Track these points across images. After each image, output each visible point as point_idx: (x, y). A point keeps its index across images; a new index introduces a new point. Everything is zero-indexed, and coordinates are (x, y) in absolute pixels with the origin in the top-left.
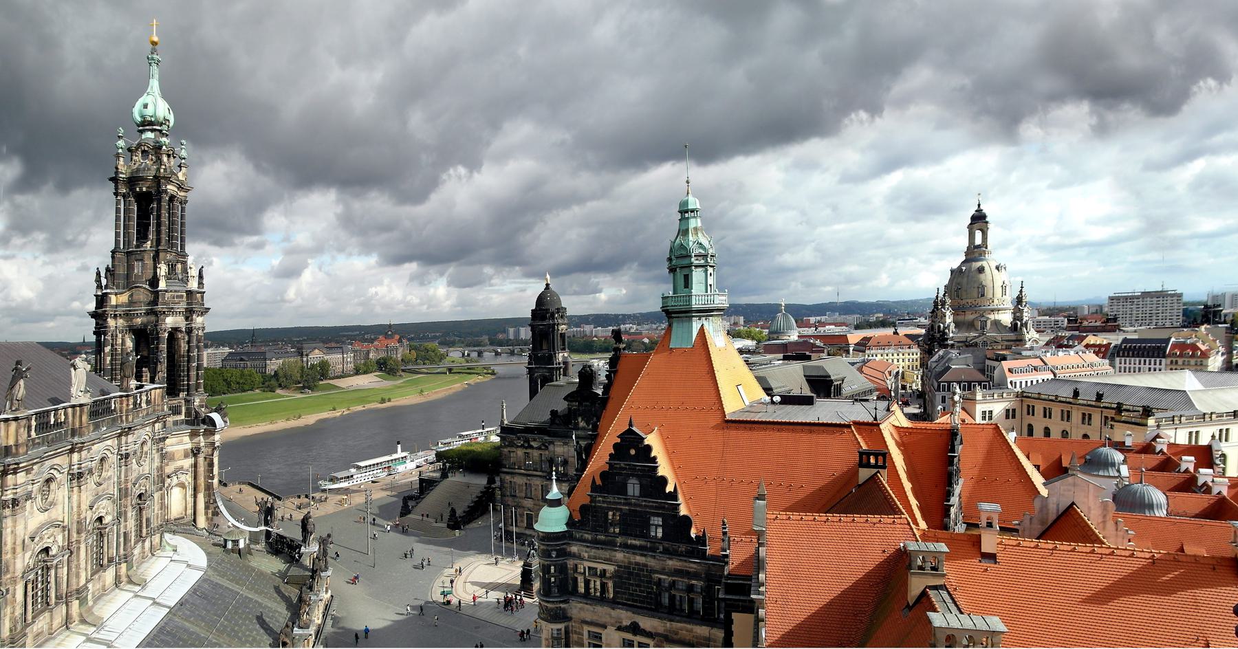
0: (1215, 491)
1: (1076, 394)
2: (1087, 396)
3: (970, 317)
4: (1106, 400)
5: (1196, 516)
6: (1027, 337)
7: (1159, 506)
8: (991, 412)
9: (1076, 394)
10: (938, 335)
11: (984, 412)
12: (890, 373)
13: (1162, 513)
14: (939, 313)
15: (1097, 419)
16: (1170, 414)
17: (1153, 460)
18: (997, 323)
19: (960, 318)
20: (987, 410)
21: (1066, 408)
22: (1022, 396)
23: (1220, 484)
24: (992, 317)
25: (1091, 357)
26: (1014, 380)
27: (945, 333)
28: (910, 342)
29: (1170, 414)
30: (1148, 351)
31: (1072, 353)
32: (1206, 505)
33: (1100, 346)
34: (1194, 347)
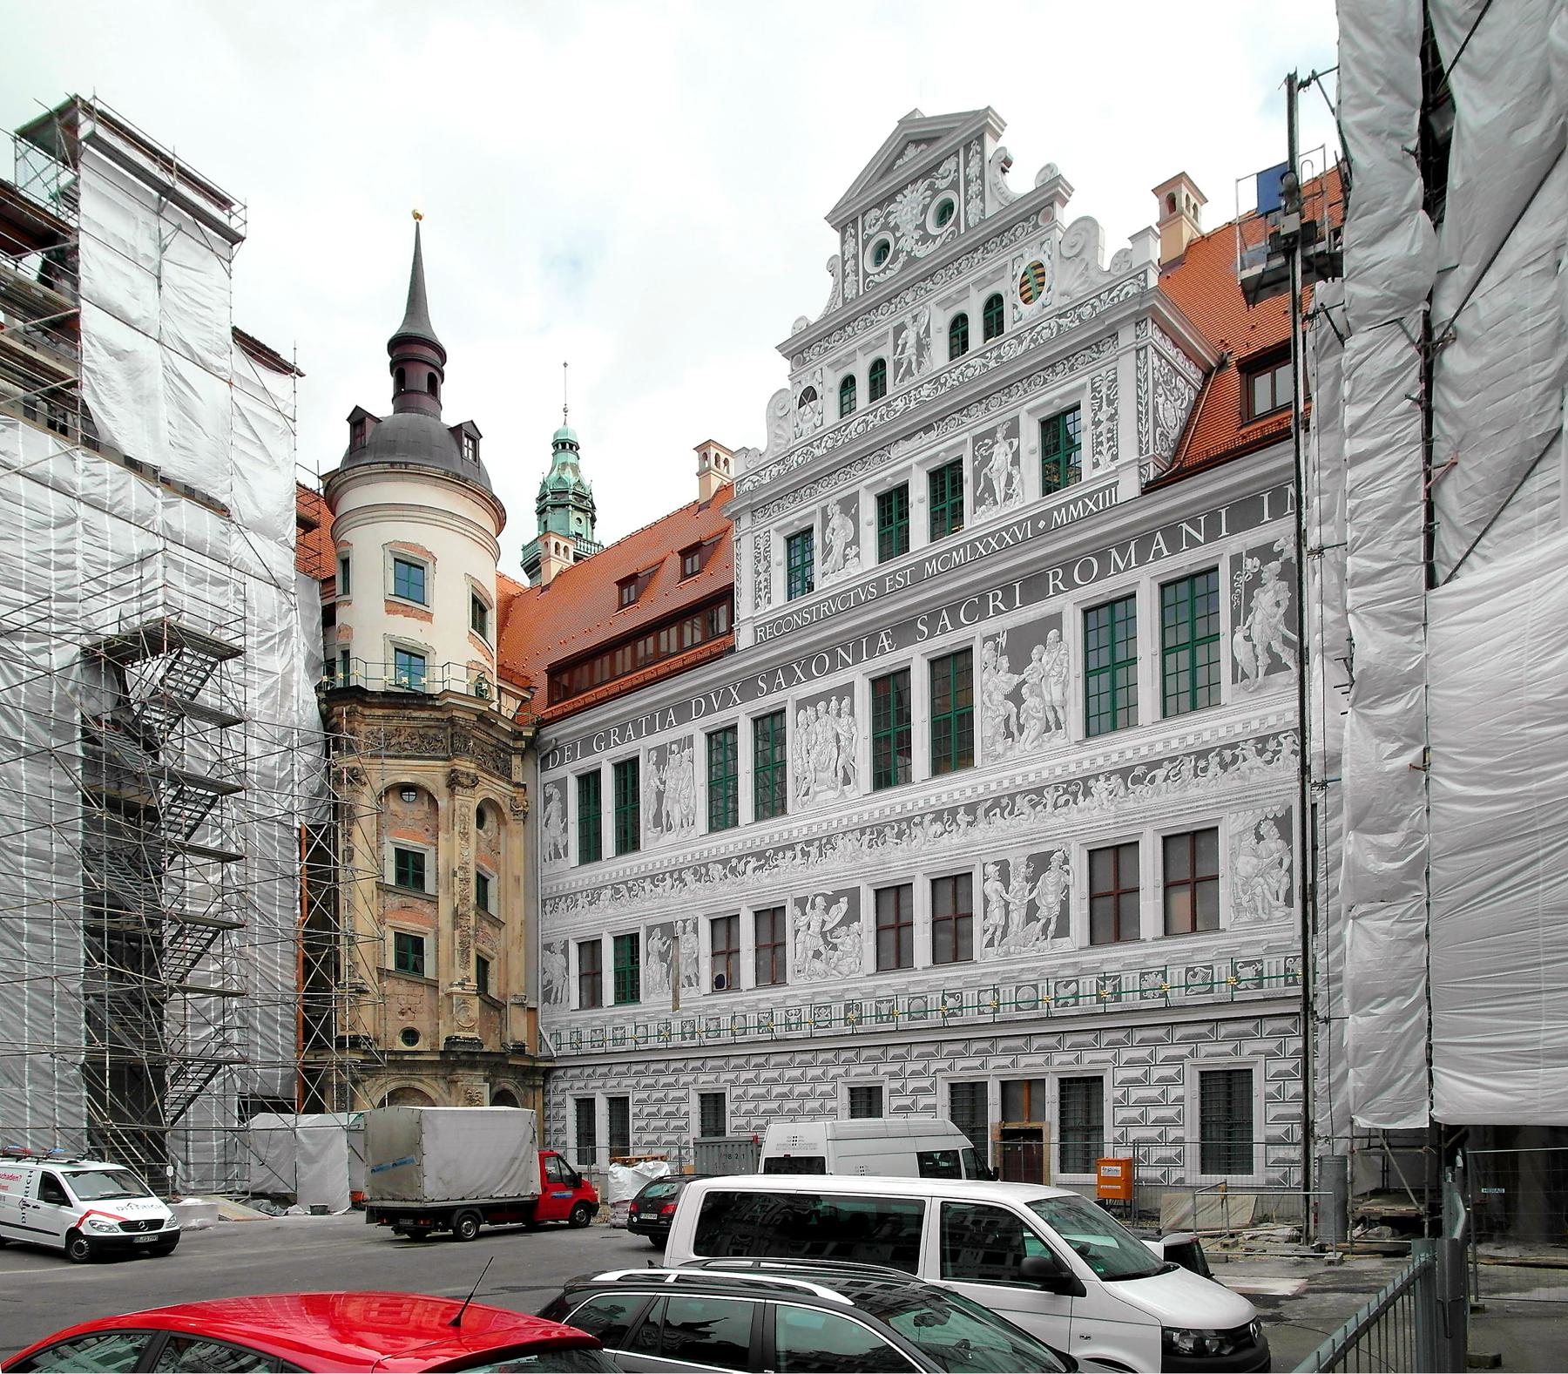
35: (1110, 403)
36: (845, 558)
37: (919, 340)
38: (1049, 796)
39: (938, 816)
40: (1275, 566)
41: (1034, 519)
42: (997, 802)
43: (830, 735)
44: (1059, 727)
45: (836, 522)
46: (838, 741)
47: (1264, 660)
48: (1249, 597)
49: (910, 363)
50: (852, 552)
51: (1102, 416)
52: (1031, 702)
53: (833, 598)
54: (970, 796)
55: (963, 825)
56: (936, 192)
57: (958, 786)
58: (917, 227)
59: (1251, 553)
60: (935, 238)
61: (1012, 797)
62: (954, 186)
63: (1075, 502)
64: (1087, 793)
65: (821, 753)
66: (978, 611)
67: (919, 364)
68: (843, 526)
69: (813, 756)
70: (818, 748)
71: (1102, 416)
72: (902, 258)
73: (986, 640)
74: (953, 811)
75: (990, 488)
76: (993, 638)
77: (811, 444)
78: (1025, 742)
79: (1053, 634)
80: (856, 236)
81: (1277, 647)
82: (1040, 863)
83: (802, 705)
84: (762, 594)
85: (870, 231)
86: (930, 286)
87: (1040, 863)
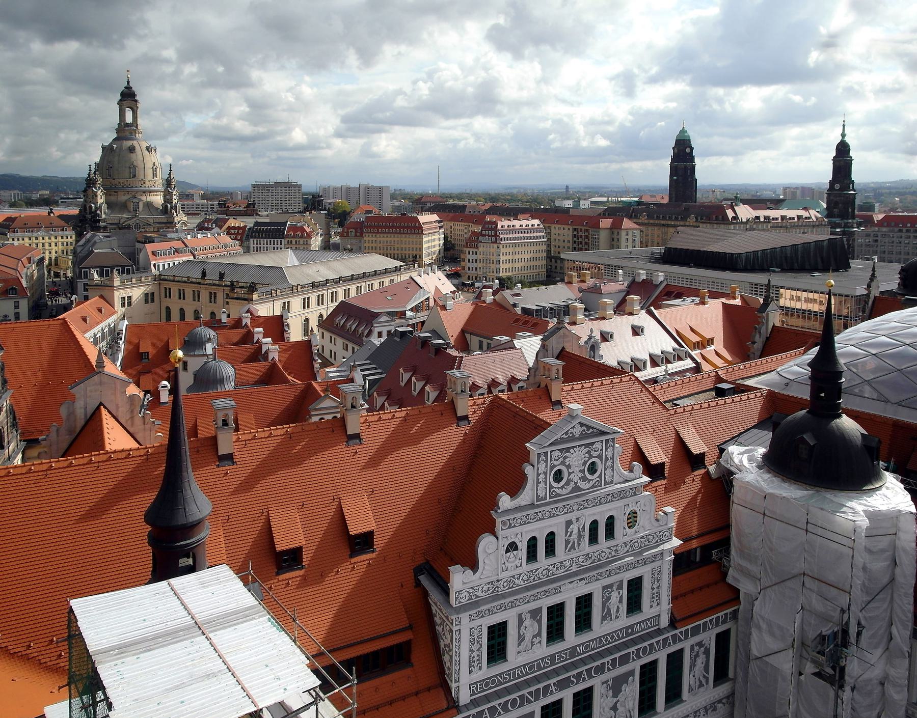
0: (270, 358)
1: (204, 274)
2: (213, 276)
4: (227, 279)
6: (177, 219)
7: (229, 380)
8: (130, 298)
9: (204, 274)
10: (89, 216)
11: (123, 299)
12: (29, 260)
15: (220, 296)
16: (268, 289)
17: (238, 333)
20: (126, 295)
21: (196, 288)
22: (160, 279)
23: (273, 351)
24: (144, 198)
25: (227, 239)
28: (63, 223)
29: (268, 289)
30: (273, 233)
31: (209, 235)
33: (239, 228)
34: (302, 229)
35: (658, 581)
36: (532, 645)
37: (579, 532)
40: (702, 649)
41: (627, 628)
45: (527, 622)
47: (698, 683)
49: (574, 543)
50: (536, 640)
52: (621, 709)
53: (524, 666)
56: (591, 457)
58: (580, 471)
60: (589, 481)
62: (600, 457)
63: (643, 621)
66: (600, 670)
67: (579, 545)
68: (532, 626)
71: (655, 586)
72: (572, 485)
73: (603, 683)
75: (609, 613)
76: (606, 682)
77: (513, 577)
79: (631, 678)
80: (546, 462)
84: (475, 664)
85: (556, 463)
86: (586, 505)
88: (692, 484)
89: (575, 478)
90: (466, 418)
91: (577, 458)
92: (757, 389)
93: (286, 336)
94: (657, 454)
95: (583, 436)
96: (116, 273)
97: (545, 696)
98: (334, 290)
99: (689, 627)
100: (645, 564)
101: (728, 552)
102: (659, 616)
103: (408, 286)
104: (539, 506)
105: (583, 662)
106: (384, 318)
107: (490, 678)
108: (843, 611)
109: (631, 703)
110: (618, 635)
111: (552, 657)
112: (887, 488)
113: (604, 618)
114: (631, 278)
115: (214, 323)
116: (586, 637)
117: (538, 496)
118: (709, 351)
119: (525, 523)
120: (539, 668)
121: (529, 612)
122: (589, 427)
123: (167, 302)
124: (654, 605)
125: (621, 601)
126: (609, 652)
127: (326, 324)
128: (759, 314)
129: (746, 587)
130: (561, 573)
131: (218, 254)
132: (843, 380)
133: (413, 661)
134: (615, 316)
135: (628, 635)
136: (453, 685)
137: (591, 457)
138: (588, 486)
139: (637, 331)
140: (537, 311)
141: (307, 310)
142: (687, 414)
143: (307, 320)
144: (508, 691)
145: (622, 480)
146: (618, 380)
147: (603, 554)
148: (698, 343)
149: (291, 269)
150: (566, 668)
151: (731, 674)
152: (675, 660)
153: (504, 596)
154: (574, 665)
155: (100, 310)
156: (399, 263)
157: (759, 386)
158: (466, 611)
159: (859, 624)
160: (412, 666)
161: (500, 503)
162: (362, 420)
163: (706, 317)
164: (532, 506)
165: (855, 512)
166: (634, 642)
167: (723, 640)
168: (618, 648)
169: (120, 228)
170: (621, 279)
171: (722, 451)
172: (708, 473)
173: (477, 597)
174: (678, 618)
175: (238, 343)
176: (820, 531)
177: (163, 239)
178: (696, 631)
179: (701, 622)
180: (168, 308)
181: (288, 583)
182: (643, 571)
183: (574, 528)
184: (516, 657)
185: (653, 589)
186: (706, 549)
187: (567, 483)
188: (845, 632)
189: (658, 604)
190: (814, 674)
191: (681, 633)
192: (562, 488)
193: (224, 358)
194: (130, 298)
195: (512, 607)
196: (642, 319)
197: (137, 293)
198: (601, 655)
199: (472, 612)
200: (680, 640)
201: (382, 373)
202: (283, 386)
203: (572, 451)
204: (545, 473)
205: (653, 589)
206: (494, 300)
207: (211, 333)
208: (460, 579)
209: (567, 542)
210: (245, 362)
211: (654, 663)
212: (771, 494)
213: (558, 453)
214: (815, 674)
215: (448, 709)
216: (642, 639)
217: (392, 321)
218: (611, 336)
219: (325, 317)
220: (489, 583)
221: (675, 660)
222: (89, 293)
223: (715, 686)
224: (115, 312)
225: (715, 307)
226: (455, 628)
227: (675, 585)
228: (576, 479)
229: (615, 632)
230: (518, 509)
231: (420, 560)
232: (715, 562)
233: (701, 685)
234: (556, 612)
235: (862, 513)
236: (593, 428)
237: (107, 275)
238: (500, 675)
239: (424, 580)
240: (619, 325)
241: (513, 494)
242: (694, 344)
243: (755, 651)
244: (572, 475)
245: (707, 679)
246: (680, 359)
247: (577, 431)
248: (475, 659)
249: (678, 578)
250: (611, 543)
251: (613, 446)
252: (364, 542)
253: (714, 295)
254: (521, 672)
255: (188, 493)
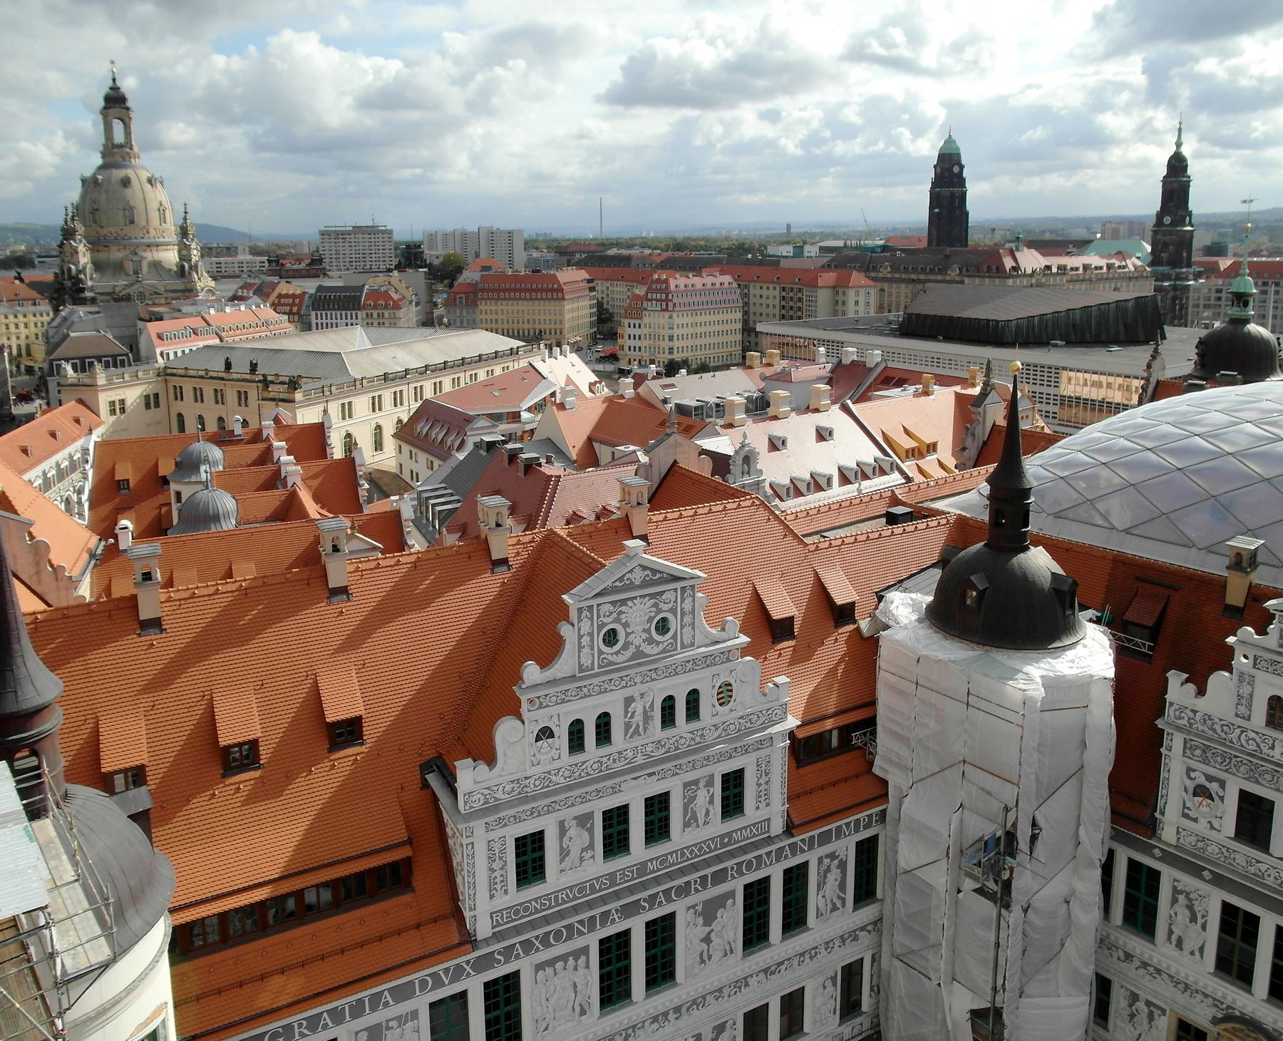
0: (289, 484)
1: (228, 365)
2: (240, 368)
3: (116, 254)
4: (260, 371)
5: (268, 520)
6: (199, 285)
7: (227, 515)
8: (122, 402)
9: (228, 365)
10: (68, 284)
13: (229, 525)
14: (67, 248)
15: (253, 395)
18: (157, 266)
19: (102, 256)
21: (219, 385)
22: (165, 374)
24: (151, 256)
25: (267, 312)
26: (165, 349)
27: (80, 281)
28: (34, 294)
30: (342, 304)
31: (243, 308)
32: (277, 504)
33: (294, 296)
34: (386, 296)
35: (767, 774)
37: (645, 712)
38: (726, 992)
39: (655, 1019)
40: (836, 862)
41: (722, 837)
42: (694, 1002)
43: (568, 984)
44: (732, 952)
45: (573, 831)
46: (575, 986)
47: (830, 906)
48: (825, 877)
49: (638, 726)
51: (762, 781)
53: (571, 888)
54: (677, 1002)
55: (672, 1020)
56: (660, 611)
57: (666, 998)
58: (644, 630)
59: (827, 856)
60: (658, 643)
61: (704, 997)
62: (673, 611)
63: (745, 828)
64: (747, 985)
65: (559, 999)
66: (684, 890)
67: (645, 729)
69: (552, 1001)
70: (556, 995)
71: (762, 781)
73: (689, 909)
74: (665, 1014)
76: (693, 907)
77: (549, 773)
78: (711, 965)
79: (730, 902)
80: (591, 619)
81: (835, 900)
82: (720, 1029)
83: (539, 967)
84: (498, 887)
85: (605, 620)
86: (654, 676)
87: (720, 1029)
88: (834, 648)
89: (637, 639)
90: (504, 561)
91: (638, 614)
92: (943, 513)
93: (328, 451)
94: (782, 605)
95: (645, 584)
96: (98, 367)
97: (603, 925)
98: (418, 385)
99: (815, 833)
100: (746, 752)
101: (874, 733)
102: (769, 820)
103: (525, 376)
104: (581, 679)
105: (657, 881)
106: (483, 423)
107: (520, 904)
108: (1007, 809)
109: (731, 934)
110: (708, 846)
111: (612, 876)
112: (1085, 646)
113: (686, 825)
114: (835, 360)
115: (223, 438)
116: (661, 849)
117: (580, 666)
118: (929, 463)
119: (563, 702)
120: (593, 891)
121: (575, 818)
122: (654, 571)
123: (178, 407)
124: (762, 805)
125: (711, 801)
126: (695, 868)
127: (405, 432)
128: (973, 409)
129: (896, 780)
130: (619, 766)
131: (257, 336)
132: (1032, 499)
133: (414, 884)
134: (793, 414)
135: (723, 845)
136: (467, 914)
137: (659, 611)
138: (656, 650)
139: (823, 435)
140: (696, 408)
141: (378, 414)
142: (834, 551)
143: (379, 427)
144: (547, 920)
145: (708, 641)
146: (735, 505)
147: (682, 741)
148: (913, 450)
149: (354, 356)
150: (631, 890)
151: (879, 894)
152: (796, 879)
153: (534, 798)
154: (644, 886)
155: (77, 421)
156: (516, 343)
157: (946, 509)
158: (478, 818)
159: (1034, 824)
160: (413, 891)
161: (525, 676)
162: (352, 568)
163: (928, 414)
164: (573, 678)
165: (1029, 679)
166: (731, 854)
167: (867, 851)
168: (708, 865)
169: (115, 300)
170: (823, 360)
171: (880, 598)
172: (858, 630)
173: (497, 799)
174: (797, 823)
175: (254, 464)
176: (983, 705)
177: (176, 315)
178: (825, 838)
179: (833, 826)
180: (180, 416)
181: (239, 788)
182: (746, 762)
183: (638, 707)
184: (557, 876)
185: (759, 785)
186: (845, 731)
187: (626, 646)
188: (1011, 836)
189: (768, 805)
190: (974, 891)
191: (803, 841)
192: (617, 653)
193: (225, 488)
194: (122, 402)
195: (549, 812)
196: (834, 417)
197: (133, 395)
198: (682, 872)
199: (490, 819)
200: (803, 851)
201: (458, 501)
202: (297, 523)
203: (630, 603)
204: (591, 635)
205: (759, 785)
206: (638, 395)
207: (216, 453)
208: (468, 775)
209: (628, 726)
210: (258, 490)
211: (764, 883)
212: (926, 657)
213: (609, 607)
214: (977, 891)
215: (460, 944)
216: (744, 850)
217: (494, 426)
218: (784, 443)
219: (405, 420)
220: (513, 782)
221: (796, 879)
222: (63, 396)
223: (855, 909)
224: (102, 423)
225: (944, 398)
226: (465, 841)
227: (792, 781)
228: (637, 642)
229: (704, 842)
230: (552, 682)
231: (429, 753)
232: (860, 748)
233: (835, 908)
234: (616, 820)
235: (1039, 680)
236: (661, 572)
237: (83, 370)
238: (535, 900)
239: (433, 779)
240: (797, 428)
241: (545, 663)
242: (907, 451)
243: (903, 864)
244: (631, 638)
245: (843, 901)
246: (883, 472)
247: (638, 576)
248: (498, 881)
249: (803, 771)
250: (695, 725)
251: (694, 596)
252: (349, 731)
253: (945, 381)
254: (567, 895)
255: (21, 672)
